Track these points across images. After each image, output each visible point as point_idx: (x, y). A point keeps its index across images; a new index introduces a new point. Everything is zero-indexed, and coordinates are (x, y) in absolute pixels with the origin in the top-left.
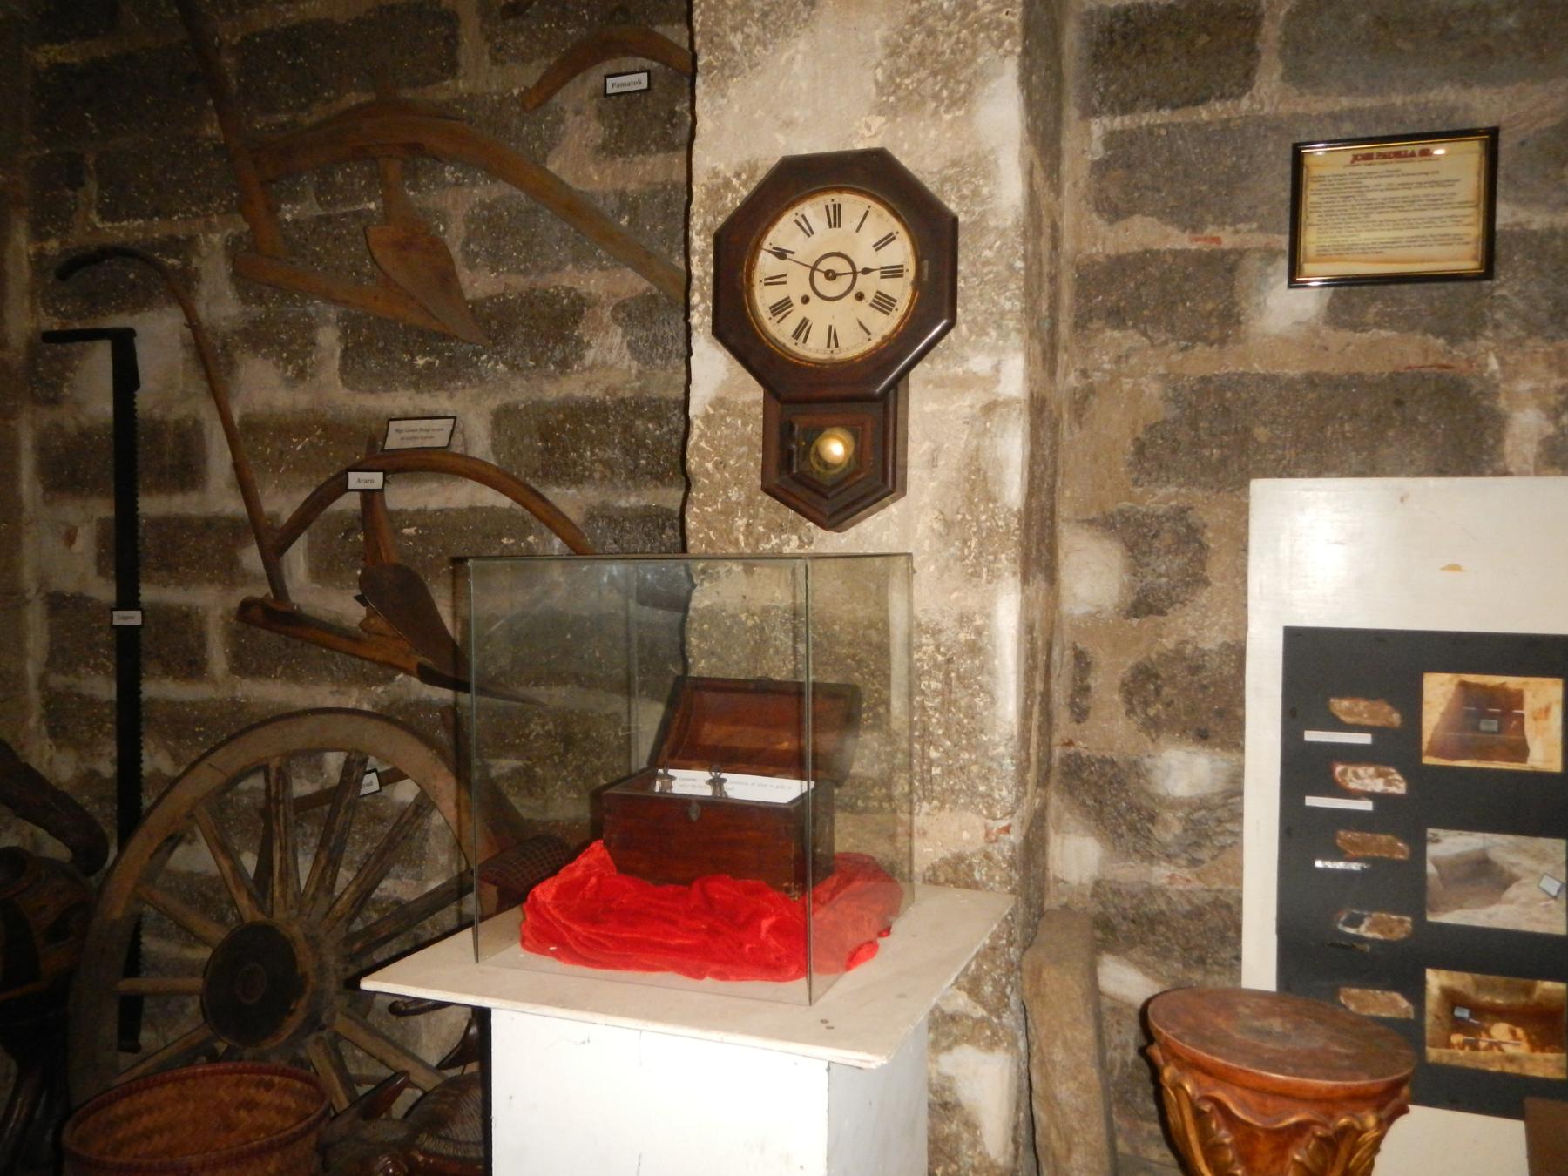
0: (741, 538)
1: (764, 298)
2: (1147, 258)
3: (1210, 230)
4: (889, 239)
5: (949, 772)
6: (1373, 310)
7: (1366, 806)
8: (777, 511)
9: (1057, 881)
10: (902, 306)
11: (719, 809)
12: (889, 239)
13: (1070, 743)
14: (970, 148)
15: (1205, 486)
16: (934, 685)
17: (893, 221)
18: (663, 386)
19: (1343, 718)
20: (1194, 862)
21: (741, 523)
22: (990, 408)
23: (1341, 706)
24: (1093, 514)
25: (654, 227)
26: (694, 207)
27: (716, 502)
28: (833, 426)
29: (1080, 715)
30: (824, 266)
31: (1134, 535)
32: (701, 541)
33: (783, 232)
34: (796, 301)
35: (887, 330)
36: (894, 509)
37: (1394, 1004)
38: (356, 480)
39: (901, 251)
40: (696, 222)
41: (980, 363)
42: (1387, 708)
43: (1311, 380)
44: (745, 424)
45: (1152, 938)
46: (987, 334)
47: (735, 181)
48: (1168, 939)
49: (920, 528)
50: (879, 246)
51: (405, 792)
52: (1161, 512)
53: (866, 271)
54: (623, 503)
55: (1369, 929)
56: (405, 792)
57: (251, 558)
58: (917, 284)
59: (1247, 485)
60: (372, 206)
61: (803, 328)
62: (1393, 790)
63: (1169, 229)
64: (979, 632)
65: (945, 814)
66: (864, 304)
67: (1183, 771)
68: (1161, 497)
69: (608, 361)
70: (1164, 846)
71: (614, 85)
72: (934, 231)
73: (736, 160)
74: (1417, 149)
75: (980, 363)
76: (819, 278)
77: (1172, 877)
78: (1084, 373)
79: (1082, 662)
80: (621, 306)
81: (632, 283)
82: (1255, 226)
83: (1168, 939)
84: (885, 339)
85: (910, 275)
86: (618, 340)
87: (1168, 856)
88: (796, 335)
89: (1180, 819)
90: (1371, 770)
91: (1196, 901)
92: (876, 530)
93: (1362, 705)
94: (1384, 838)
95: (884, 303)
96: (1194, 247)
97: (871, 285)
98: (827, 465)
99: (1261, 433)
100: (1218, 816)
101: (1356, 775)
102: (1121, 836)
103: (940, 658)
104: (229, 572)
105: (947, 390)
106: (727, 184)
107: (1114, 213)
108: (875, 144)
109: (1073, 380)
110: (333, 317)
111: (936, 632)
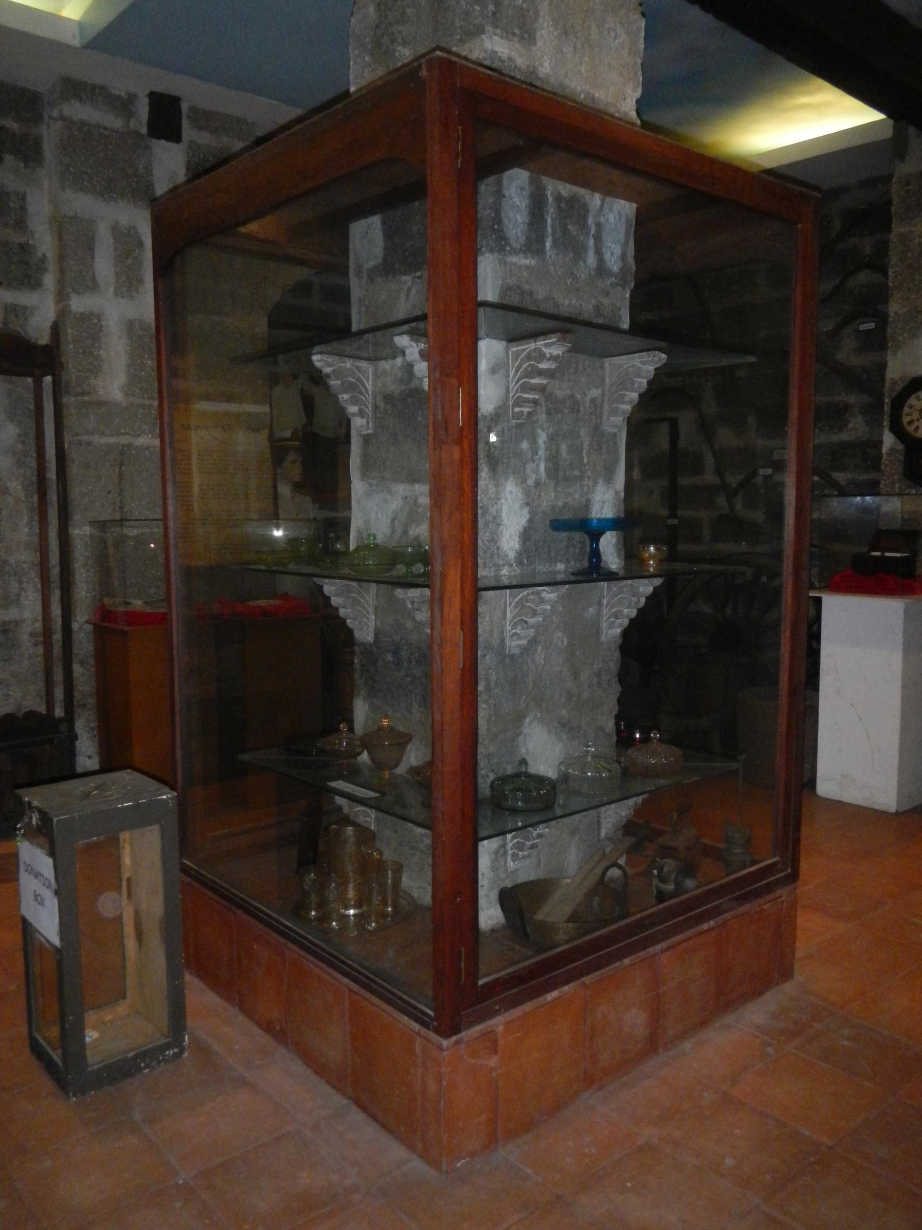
1: (906, 420)
11: (882, 558)
21: (897, 486)
38: (761, 472)
54: (860, 478)
57: (721, 500)
69: (856, 427)
71: (862, 327)
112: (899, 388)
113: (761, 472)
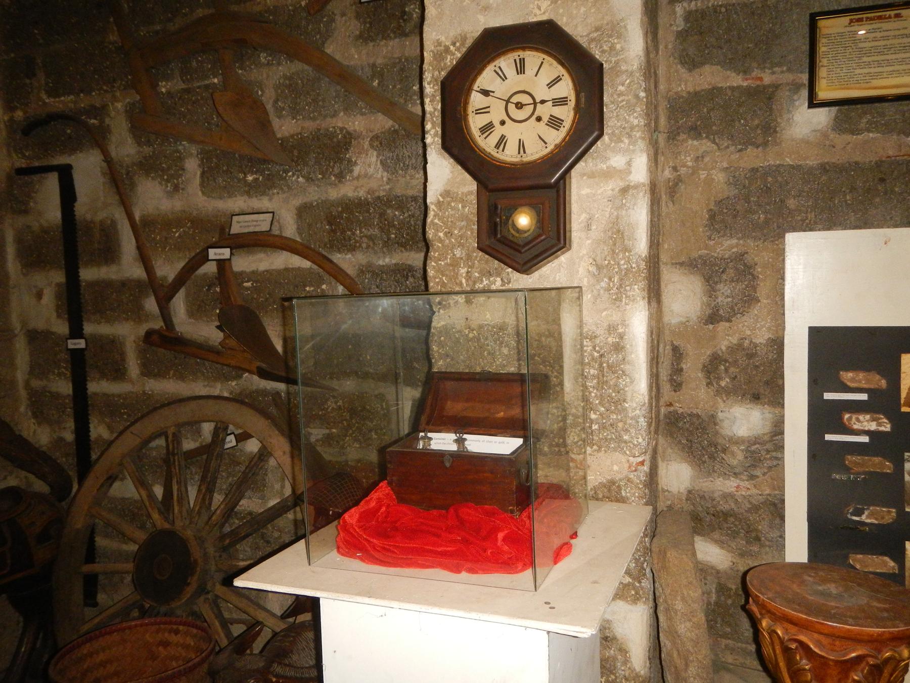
0: (464, 281)
1: (475, 123)
2: (714, 93)
3: (756, 73)
4: (558, 80)
5: (603, 427)
6: (865, 120)
7: (865, 439)
8: (487, 262)
9: (664, 491)
10: (567, 124)
11: (463, 459)
12: (558, 80)
13: (671, 405)
14: (608, 18)
15: (755, 238)
16: (592, 371)
17: (560, 68)
18: (407, 185)
19: (849, 384)
20: (752, 477)
21: (463, 271)
22: (625, 190)
23: (847, 376)
24: (683, 259)
25: (394, 87)
26: (425, 66)
27: (446, 258)
28: (522, 205)
29: (677, 386)
30: (515, 99)
31: (709, 271)
32: (438, 284)
33: (486, 78)
34: (496, 123)
35: (558, 141)
36: (563, 258)
37: (885, 564)
38: (213, 253)
39: (566, 88)
40: (427, 76)
41: (617, 161)
42: (878, 377)
43: (824, 168)
44: (463, 207)
45: (725, 525)
46: (622, 141)
47: (452, 47)
48: (735, 525)
49: (581, 270)
50: (550, 85)
51: (252, 446)
52: (727, 256)
53: (543, 102)
54: (381, 263)
55: (868, 517)
56: (252, 446)
57: (151, 304)
58: (577, 108)
59: (784, 237)
60: (216, 81)
61: (502, 142)
62: (882, 429)
63: (729, 72)
64: (621, 337)
65: (602, 454)
66: (542, 124)
67: (743, 421)
68: (727, 246)
69: (368, 174)
70: (733, 467)
72: (587, 72)
73: (452, 34)
74: (893, 13)
75: (617, 161)
76: (511, 107)
77: (738, 487)
78: (675, 169)
79: (677, 353)
80: (376, 137)
81: (382, 123)
82: (785, 68)
83: (735, 525)
84: (557, 146)
85: (572, 103)
86: (374, 159)
87: (735, 474)
88: (497, 146)
89: (742, 451)
90: (868, 417)
91: (754, 502)
92: (552, 273)
93: (861, 375)
94: (877, 460)
95: (555, 123)
96: (745, 84)
97: (545, 111)
98: (518, 230)
99: (792, 203)
100: (767, 450)
101: (858, 420)
102: (704, 462)
103: (596, 354)
104: (137, 314)
105: (596, 180)
106: (447, 50)
107: (692, 64)
108: (544, 18)
109: (668, 173)
110: (194, 152)
111: (593, 338)
112: (450, 61)
113: (213, 253)
